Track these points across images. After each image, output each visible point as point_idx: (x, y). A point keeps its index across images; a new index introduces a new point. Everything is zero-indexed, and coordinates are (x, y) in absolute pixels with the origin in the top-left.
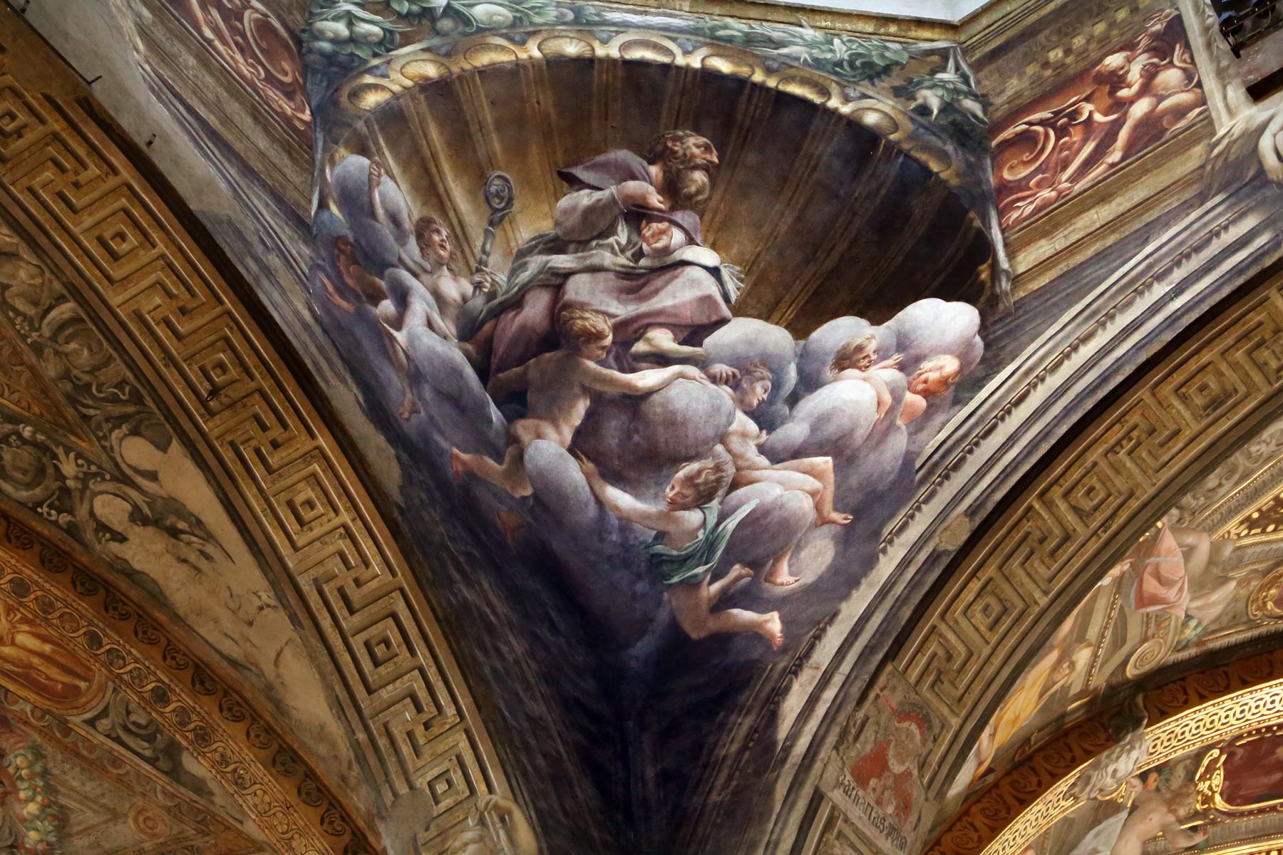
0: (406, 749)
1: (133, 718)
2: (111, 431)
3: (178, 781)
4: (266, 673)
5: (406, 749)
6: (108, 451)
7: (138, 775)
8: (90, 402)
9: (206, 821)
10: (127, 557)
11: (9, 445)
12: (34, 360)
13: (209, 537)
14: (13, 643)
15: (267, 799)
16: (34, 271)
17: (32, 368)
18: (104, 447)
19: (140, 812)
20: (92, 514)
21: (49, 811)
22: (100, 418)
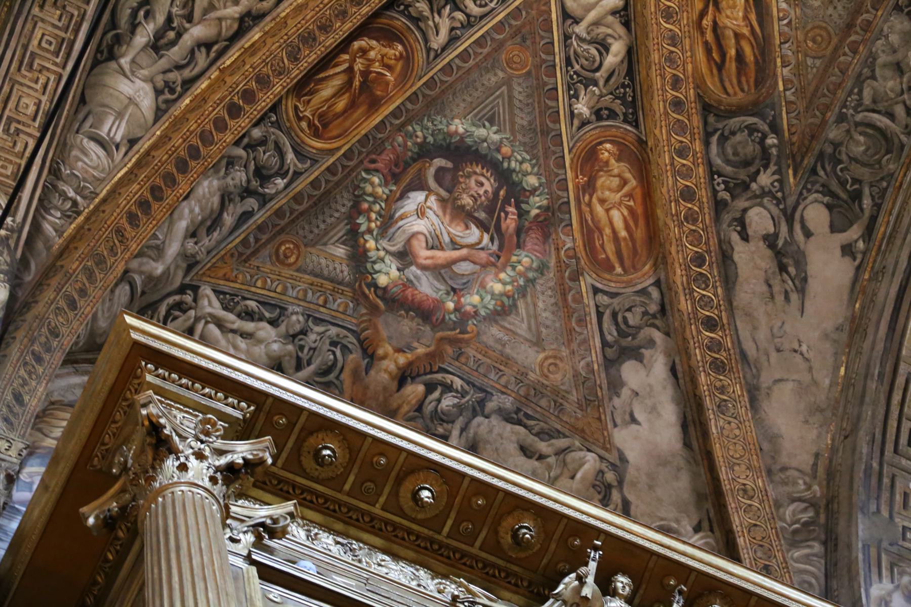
0: (898, 498)
1: (629, 315)
2: (817, 192)
3: (607, 369)
4: (762, 379)
5: (898, 498)
6: (801, 197)
7: (585, 341)
8: (828, 168)
9: (592, 402)
10: (736, 248)
11: (750, 135)
12: (832, 119)
13: (802, 291)
14: (607, 211)
15: (737, 432)
16: (898, 89)
17: (824, 122)
18: (801, 194)
19: (555, 357)
20: (745, 211)
21: (505, 299)
22: (822, 181)
